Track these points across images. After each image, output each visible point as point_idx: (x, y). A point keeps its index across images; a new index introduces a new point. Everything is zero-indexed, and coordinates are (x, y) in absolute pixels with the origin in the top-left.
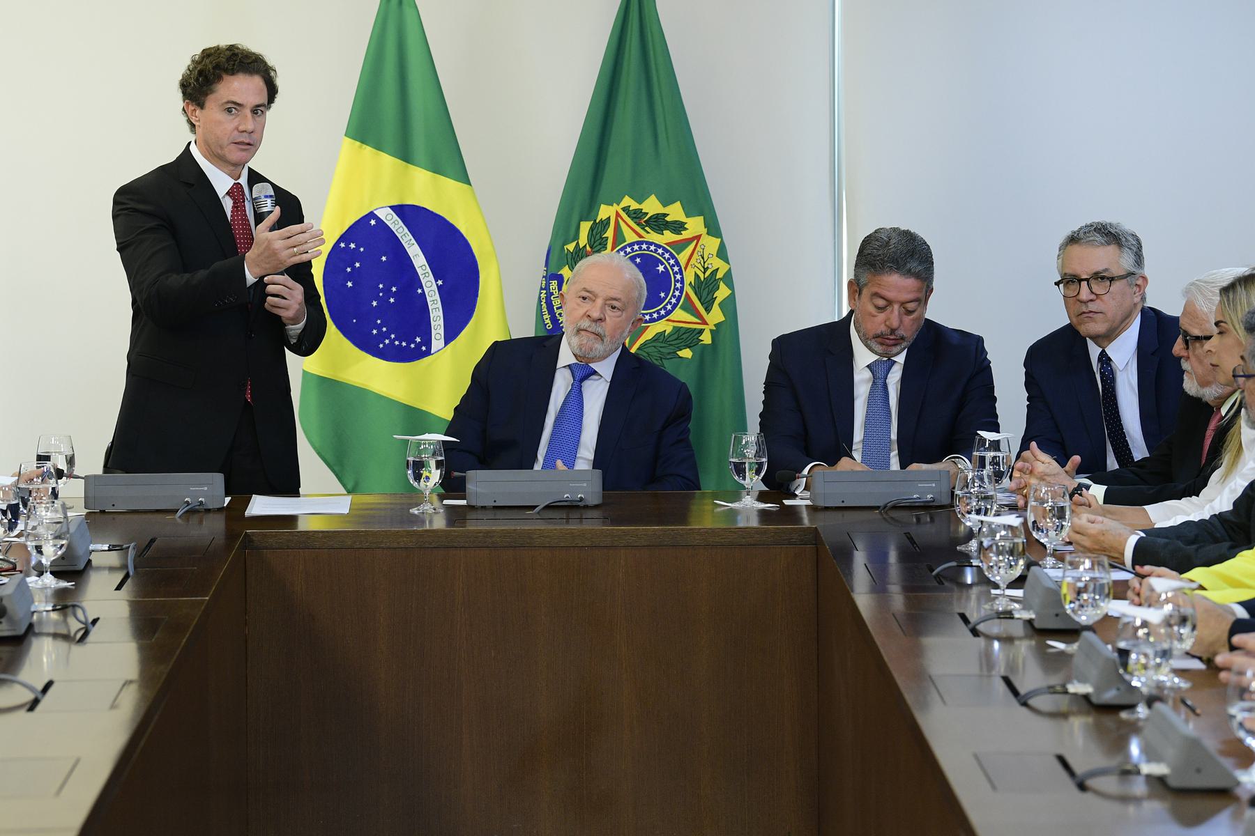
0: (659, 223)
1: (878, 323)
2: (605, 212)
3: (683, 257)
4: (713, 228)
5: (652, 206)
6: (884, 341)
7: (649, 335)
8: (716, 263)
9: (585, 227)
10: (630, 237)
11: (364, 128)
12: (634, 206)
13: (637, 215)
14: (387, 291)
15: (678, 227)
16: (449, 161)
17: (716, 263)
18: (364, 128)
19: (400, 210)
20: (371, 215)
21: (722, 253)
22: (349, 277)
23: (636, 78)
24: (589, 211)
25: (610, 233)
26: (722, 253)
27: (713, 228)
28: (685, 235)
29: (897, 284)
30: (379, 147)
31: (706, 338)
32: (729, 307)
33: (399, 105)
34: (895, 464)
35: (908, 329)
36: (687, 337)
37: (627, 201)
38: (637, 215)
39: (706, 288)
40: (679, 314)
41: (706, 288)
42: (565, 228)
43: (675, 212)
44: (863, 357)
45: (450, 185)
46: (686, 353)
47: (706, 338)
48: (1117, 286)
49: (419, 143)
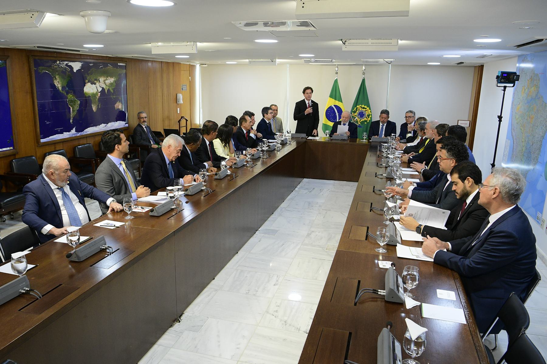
0: (364, 108)
1: (382, 120)
4: (370, 109)
5: (363, 106)
6: (383, 122)
23: (362, 91)
24: (356, 107)
27: (370, 109)
29: (384, 115)
33: (335, 93)
34: (383, 136)
35: (385, 120)
36: (366, 121)
39: (368, 116)
42: (353, 108)
43: (366, 107)
44: (381, 124)
49: (337, 98)
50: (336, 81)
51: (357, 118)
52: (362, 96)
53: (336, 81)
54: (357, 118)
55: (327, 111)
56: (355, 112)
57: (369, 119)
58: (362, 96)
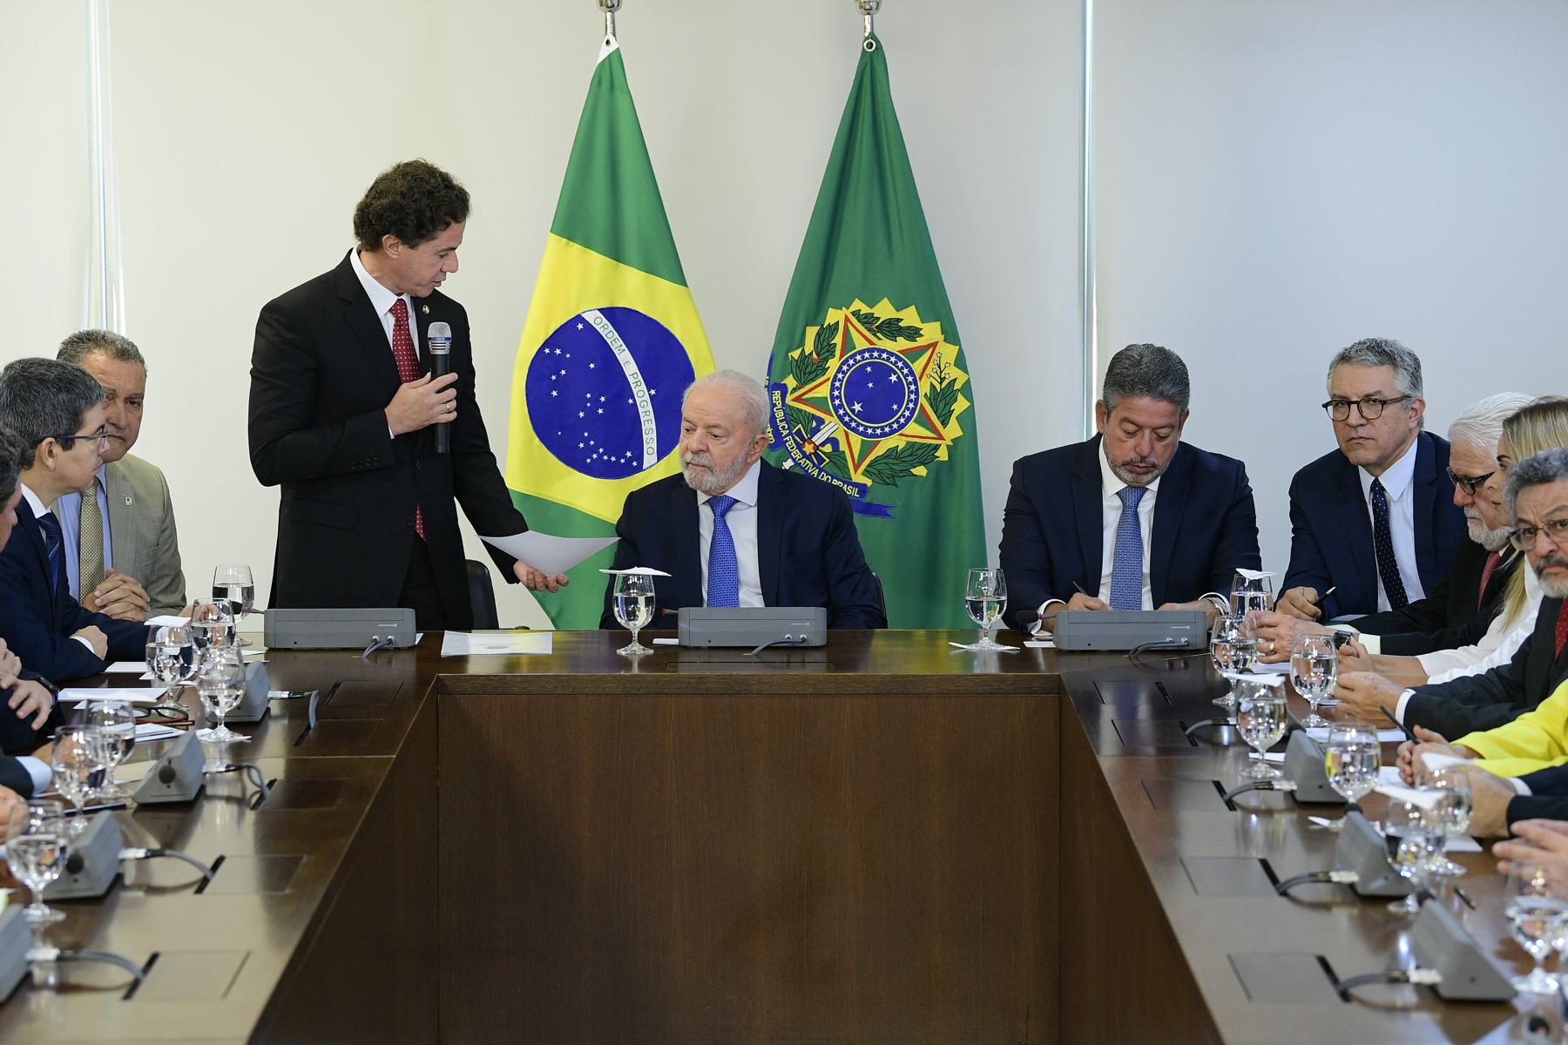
0: (892, 329)
2: (833, 316)
3: (917, 367)
5: (884, 310)
7: (880, 451)
8: (953, 372)
9: (812, 332)
10: (860, 344)
11: (572, 223)
12: (865, 310)
13: (867, 320)
14: (595, 401)
15: (913, 333)
16: (663, 260)
17: (953, 372)
18: (572, 223)
19: (610, 313)
20: (579, 318)
21: (960, 362)
22: (554, 386)
24: (816, 315)
25: (838, 340)
26: (960, 362)
27: (951, 335)
28: (920, 342)
30: (587, 244)
31: (942, 454)
32: (968, 420)
36: (921, 453)
37: (857, 305)
38: (867, 320)
39: (942, 399)
40: (913, 428)
41: (942, 399)
42: (789, 334)
43: (910, 317)
45: (665, 286)
46: (920, 471)
47: (942, 454)
48: (1389, 410)
50: (610, 79)
51: (832, 427)
52: (868, 204)
53: (610, 79)
54: (832, 427)
55: (541, 369)
56: (808, 370)
57: (953, 430)
58: (868, 204)
